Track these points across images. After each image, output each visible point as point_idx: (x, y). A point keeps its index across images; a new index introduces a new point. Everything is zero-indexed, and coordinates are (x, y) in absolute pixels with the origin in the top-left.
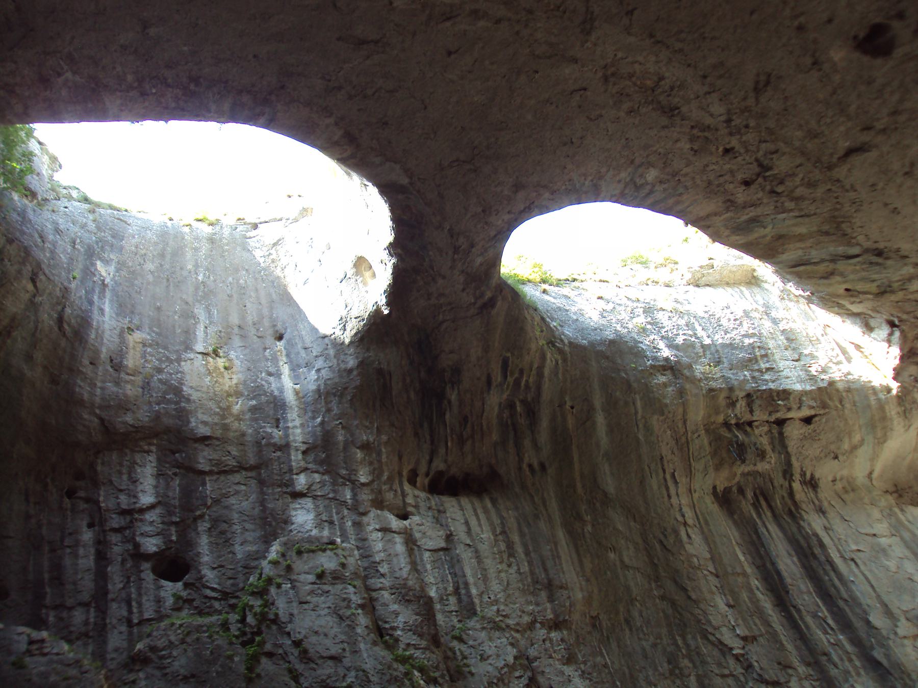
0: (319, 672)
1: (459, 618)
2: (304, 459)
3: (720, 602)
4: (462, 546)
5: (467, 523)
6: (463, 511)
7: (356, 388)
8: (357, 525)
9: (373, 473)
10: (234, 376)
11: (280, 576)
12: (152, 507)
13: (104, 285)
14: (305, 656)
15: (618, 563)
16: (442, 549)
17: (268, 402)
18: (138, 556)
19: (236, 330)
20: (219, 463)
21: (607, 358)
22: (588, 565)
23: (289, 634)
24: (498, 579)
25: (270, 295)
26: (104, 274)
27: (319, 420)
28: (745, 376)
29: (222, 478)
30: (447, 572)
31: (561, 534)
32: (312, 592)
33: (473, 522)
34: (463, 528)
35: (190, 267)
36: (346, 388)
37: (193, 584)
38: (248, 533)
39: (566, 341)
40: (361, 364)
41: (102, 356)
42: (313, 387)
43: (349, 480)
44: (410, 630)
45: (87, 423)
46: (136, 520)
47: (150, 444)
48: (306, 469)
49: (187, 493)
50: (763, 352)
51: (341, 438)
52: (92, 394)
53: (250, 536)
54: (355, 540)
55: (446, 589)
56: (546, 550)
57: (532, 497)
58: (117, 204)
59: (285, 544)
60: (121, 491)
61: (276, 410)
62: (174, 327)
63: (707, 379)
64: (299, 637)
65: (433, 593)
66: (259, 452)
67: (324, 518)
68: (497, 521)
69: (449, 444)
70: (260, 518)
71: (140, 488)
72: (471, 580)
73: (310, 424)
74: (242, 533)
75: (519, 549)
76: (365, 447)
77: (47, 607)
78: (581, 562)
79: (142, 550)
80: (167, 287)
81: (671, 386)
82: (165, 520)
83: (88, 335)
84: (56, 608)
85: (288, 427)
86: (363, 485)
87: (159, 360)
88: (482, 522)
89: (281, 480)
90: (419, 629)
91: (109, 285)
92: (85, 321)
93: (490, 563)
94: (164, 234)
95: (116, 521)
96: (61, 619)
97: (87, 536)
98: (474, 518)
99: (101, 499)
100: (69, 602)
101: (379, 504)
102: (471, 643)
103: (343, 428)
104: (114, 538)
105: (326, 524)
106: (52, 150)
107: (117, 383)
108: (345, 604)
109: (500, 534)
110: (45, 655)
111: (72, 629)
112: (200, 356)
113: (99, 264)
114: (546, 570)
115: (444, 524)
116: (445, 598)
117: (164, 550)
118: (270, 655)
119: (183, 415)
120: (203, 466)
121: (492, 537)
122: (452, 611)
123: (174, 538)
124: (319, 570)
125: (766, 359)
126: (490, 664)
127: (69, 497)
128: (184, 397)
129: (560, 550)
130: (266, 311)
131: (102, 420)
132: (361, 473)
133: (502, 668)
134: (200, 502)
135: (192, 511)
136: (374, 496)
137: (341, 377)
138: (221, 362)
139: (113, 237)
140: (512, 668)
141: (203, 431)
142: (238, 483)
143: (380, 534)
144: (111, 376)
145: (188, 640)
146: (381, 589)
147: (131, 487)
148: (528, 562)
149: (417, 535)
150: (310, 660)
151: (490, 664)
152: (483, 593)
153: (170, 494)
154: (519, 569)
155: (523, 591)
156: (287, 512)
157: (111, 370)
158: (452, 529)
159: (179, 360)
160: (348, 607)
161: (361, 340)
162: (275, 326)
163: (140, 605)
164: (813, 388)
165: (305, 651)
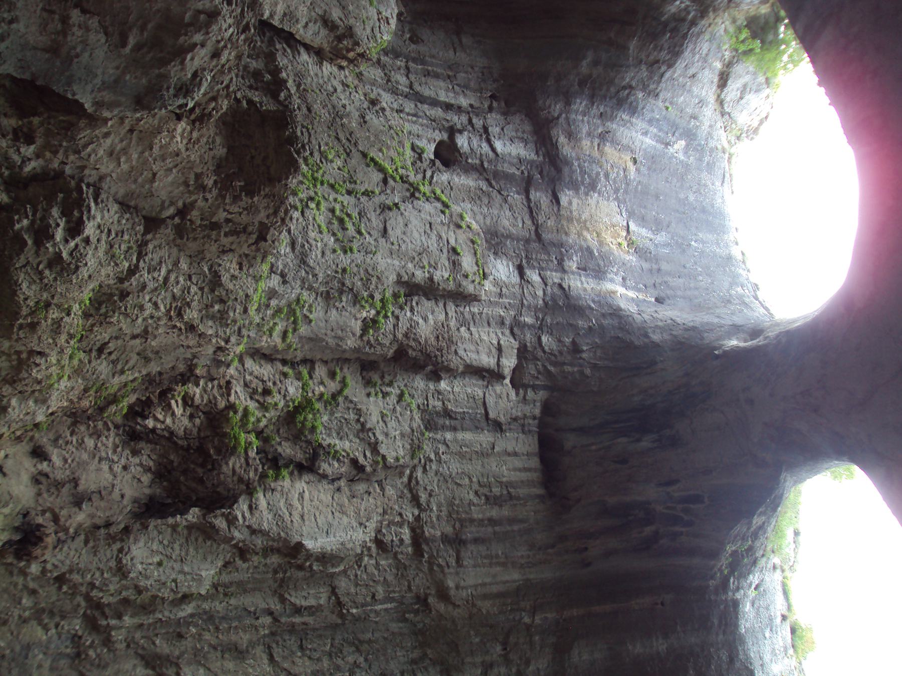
0: (373, 213)
1: (421, 407)
2: (554, 283)
4: (491, 439)
5: (515, 454)
6: (527, 455)
7: (632, 342)
9: (551, 354)
10: (614, 247)
11: (451, 216)
12: (494, 150)
13: (667, 144)
14: (385, 208)
15: (488, 658)
16: (487, 413)
17: (599, 265)
18: (452, 131)
19: (655, 267)
20: (538, 207)
21: (732, 660)
22: (486, 606)
23: (404, 202)
24: (463, 473)
25: (696, 298)
26: (676, 146)
27: (593, 305)
29: (526, 209)
30: (465, 410)
31: (515, 576)
32: (440, 237)
33: (518, 463)
34: (510, 449)
35: (701, 235)
36: (629, 333)
37: (434, 164)
38: (482, 217)
39: (738, 596)
40: (656, 345)
41: (608, 124)
42: (623, 306)
43: (541, 324)
44: (411, 326)
45: (553, 106)
46: (481, 135)
47: (544, 156)
48: (546, 285)
49: (508, 177)
52: (577, 112)
53: (480, 217)
54: (487, 314)
56: (498, 549)
57: (553, 546)
58: (734, 179)
59: (479, 234)
60: (502, 129)
61: (593, 270)
62: (645, 207)
64: (402, 208)
65: (443, 385)
66: (554, 244)
67: (504, 290)
68: (522, 492)
69: (594, 447)
70: (496, 232)
71: (508, 144)
72: (460, 435)
74: (481, 213)
75: (494, 513)
76: (575, 349)
77: (407, 62)
78: (485, 597)
79: (457, 135)
80: (678, 211)
82: (484, 157)
83: (624, 112)
84: (407, 68)
85: (580, 276)
86: (539, 338)
87: (615, 181)
88: (518, 473)
89: (532, 258)
90: (412, 336)
91: (666, 151)
92: (633, 110)
93: (475, 468)
94: (720, 215)
95: (478, 122)
96: (399, 69)
97: (464, 102)
99: (494, 115)
100: (412, 77)
101: (523, 352)
102: (398, 408)
103: (590, 327)
104: (464, 119)
105: (499, 290)
106: (762, 128)
107: (589, 134)
108: (432, 263)
109: (509, 493)
110: (379, 20)
111: (393, 73)
112: (625, 224)
113: (682, 143)
114: (476, 541)
115: (512, 427)
117: (459, 152)
118: (385, 181)
119: (575, 187)
120: (535, 195)
121: (504, 480)
122: (427, 400)
123: (470, 161)
124: (459, 250)
126: (378, 422)
127: (490, 97)
128: (589, 191)
129: (498, 569)
130: (679, 293)
131: (558, 118)
133: (374, 434)
134: (503, 186)
135: (494, 178)
136: (529, 349)
137: (639, 329)
138: (625, 244)
139: (708, 163)
140: (374, 448)
141: (564, 200)
142: (523, 222)
143: (495, 342)
144: (594, 130)
145: (392, 131)
146: (447, 314)
147: (506, 137)
148: (482, 520)
149: (498, 388)
150: (383, 211)
151: (378, 422)
152: (447, 446)
153: (506, 165)
154: (474, 505)
155: (451, 504)
156: (505, 257)
157: (600, 131)
159: (617, 199)
160: (430, 265)
161: (680, 343)
162: (668, 298)
163: (415, 122)
165: (390, 209)
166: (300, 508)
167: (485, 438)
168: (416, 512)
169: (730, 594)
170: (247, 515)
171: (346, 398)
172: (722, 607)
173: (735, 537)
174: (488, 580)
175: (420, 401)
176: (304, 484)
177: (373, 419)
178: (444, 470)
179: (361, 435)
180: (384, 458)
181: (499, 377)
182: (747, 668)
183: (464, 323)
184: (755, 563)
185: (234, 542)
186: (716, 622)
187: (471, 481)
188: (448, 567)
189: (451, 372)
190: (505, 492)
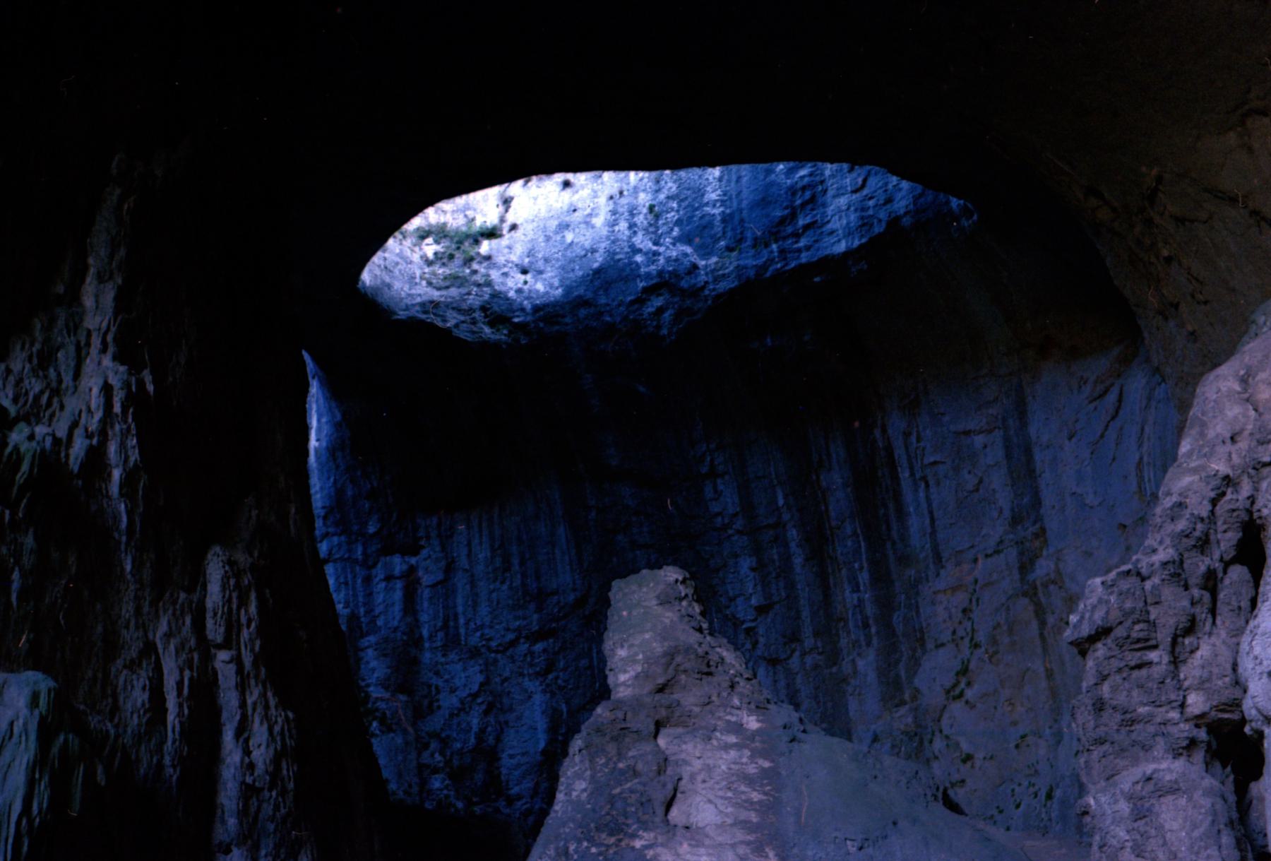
3: (746, 564)
5: (469, 544)
8: (368, 580)
27: (332, 479)
28: (772, 252)
31: (561, 530)
34: (464, 551)
50: (808, 194)
51: (349, 493)
55: (435, 626)
63: (716, 280)
72: (460, 609)
73: (327, 485)
75: (515, 561)
81: (667, 309)
98: (477, 536)
101: (387, 551)
102: (446, 677)
105: (343, 586)
116: (434, 634)
121: (489, 554)
122: (436, 648)
125: (810, 206)
132: (371, 523)
133: (466, 698)
140: (474, 696)
152: (469, 620)
154: (511, 584)
158: (455, 555)
164: (864, 240)
166: (519, 757)
167: (460, 581)
168: (522, 640)
169: (529, 318)
170: (524, 800)
171: (442, 729)
172: (541, 325)
173: (474, 333)
174: (567, 558)
175: (439, 654)
176: (503, 756)
177: (455, 701)
178: (487, 620)
179: (467, 710)
180: (482, 685)
181: (412, 569)
182: (592, 281)
183: (373, 621)
184: (496, 295)
185: (545, 806)
186: (557, 328)
187: (494, 591)
188: (559, 602)
189: (417, 624)
190: (499, 552)
